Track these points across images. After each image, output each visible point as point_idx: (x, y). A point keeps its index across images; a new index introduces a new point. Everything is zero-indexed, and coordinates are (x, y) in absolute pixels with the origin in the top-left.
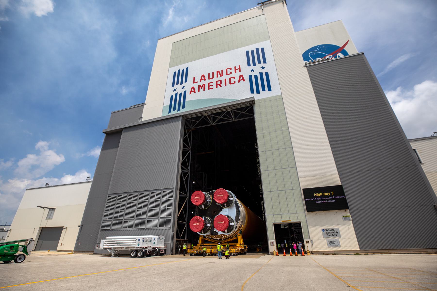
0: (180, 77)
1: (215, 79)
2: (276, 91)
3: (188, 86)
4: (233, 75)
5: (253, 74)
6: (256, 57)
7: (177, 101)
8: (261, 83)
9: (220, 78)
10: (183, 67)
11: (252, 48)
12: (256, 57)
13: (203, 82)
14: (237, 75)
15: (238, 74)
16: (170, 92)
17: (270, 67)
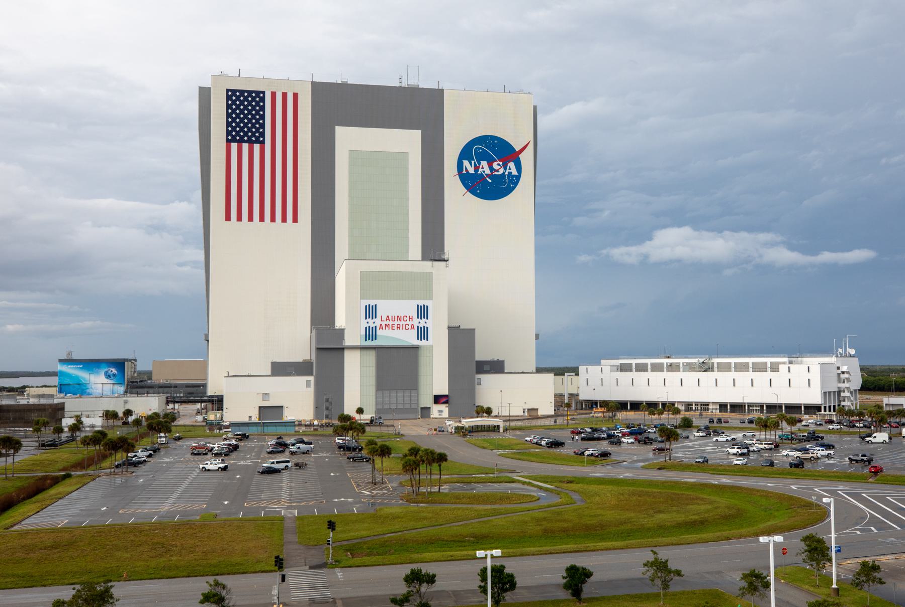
0: (371, 312)
1: (396, 323)
2: (430, 342)
3: (378, 322)
4: (408, 322)
5: (420, 326)
6: (423, 312)
7: (371, 334)
8: (423, 333)
9: (399, 322)
10: (372, 303)
11: (421, 303)
12: (423, 312)
13: (388, 322)
14: (410, 323)
15: (410, 323)
16: (364, 323)
17: (430, 323)
